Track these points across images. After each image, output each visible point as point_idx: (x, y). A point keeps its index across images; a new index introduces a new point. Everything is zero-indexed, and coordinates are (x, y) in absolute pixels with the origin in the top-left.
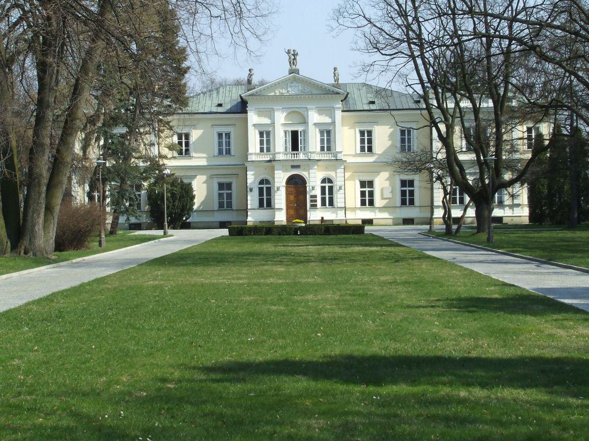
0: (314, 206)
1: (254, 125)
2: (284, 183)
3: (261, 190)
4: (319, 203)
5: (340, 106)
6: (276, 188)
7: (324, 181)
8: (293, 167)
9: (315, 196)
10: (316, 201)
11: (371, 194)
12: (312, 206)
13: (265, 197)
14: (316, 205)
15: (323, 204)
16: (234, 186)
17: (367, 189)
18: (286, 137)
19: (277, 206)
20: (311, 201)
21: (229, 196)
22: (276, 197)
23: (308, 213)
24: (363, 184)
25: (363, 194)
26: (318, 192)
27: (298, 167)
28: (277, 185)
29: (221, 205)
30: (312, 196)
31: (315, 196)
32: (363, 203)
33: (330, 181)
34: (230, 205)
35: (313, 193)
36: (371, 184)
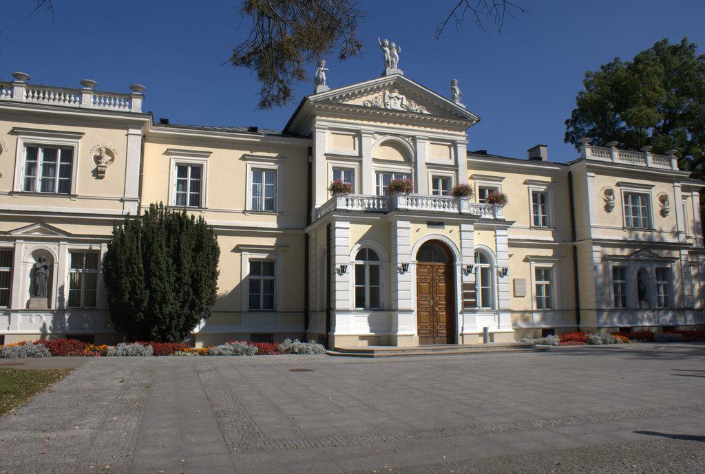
0: (470, 306)
1: (329, 156)
2: (414, 258)
3: (359, 270)
4: (480, 302)
5: (464, 139)
6: (400, 265)
8: (431, 224)
10: (474, 296)
12: (465, 305)
13: (367, 286)
14: (475, 304)
16: (278, 270)
18: (378, 183)
19: (401, 305)
20: (465, 296)
21: (270, 286)
22: (400, 286)
23: (460, 317)
27: (440, 224)
28: (401, 260)
29: (254, 304)
30: (465, 286)
34: (270, 304)
35: (470, 279)
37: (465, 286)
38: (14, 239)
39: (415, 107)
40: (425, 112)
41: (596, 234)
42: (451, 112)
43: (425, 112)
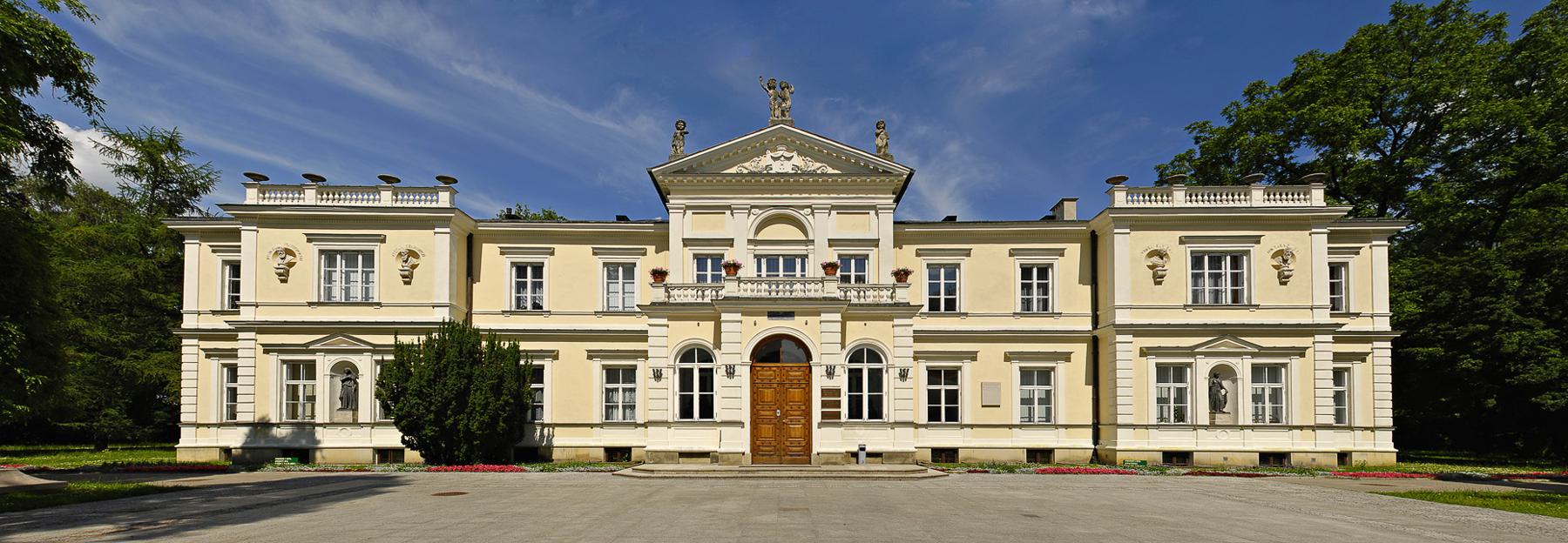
0: (830, 417)
4: (844, 409)
7: (856, 356)
9: (837, 392)
10: (838, 404)
11: (953, 397)
12: (824, 415)
14: (838, 415)
15: (855, 412)
17: (943, 388)
20: (824, 404)
24: (934, 376)
25: (933, 397)
26: (842, 381)
30: (825, 392)
31: (837, 392)
32: (934, 415)
33: (874, 356)
36: (952, 375)
37: (825, 392)
38: (314, 352)
39: (815, 166)
40: (830, 171)
41: (1122, 318)
42: (866, 166)
43: (830, 171)
